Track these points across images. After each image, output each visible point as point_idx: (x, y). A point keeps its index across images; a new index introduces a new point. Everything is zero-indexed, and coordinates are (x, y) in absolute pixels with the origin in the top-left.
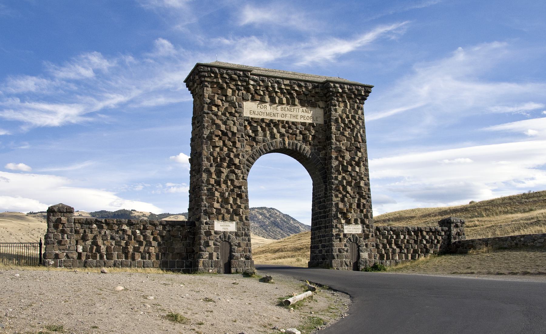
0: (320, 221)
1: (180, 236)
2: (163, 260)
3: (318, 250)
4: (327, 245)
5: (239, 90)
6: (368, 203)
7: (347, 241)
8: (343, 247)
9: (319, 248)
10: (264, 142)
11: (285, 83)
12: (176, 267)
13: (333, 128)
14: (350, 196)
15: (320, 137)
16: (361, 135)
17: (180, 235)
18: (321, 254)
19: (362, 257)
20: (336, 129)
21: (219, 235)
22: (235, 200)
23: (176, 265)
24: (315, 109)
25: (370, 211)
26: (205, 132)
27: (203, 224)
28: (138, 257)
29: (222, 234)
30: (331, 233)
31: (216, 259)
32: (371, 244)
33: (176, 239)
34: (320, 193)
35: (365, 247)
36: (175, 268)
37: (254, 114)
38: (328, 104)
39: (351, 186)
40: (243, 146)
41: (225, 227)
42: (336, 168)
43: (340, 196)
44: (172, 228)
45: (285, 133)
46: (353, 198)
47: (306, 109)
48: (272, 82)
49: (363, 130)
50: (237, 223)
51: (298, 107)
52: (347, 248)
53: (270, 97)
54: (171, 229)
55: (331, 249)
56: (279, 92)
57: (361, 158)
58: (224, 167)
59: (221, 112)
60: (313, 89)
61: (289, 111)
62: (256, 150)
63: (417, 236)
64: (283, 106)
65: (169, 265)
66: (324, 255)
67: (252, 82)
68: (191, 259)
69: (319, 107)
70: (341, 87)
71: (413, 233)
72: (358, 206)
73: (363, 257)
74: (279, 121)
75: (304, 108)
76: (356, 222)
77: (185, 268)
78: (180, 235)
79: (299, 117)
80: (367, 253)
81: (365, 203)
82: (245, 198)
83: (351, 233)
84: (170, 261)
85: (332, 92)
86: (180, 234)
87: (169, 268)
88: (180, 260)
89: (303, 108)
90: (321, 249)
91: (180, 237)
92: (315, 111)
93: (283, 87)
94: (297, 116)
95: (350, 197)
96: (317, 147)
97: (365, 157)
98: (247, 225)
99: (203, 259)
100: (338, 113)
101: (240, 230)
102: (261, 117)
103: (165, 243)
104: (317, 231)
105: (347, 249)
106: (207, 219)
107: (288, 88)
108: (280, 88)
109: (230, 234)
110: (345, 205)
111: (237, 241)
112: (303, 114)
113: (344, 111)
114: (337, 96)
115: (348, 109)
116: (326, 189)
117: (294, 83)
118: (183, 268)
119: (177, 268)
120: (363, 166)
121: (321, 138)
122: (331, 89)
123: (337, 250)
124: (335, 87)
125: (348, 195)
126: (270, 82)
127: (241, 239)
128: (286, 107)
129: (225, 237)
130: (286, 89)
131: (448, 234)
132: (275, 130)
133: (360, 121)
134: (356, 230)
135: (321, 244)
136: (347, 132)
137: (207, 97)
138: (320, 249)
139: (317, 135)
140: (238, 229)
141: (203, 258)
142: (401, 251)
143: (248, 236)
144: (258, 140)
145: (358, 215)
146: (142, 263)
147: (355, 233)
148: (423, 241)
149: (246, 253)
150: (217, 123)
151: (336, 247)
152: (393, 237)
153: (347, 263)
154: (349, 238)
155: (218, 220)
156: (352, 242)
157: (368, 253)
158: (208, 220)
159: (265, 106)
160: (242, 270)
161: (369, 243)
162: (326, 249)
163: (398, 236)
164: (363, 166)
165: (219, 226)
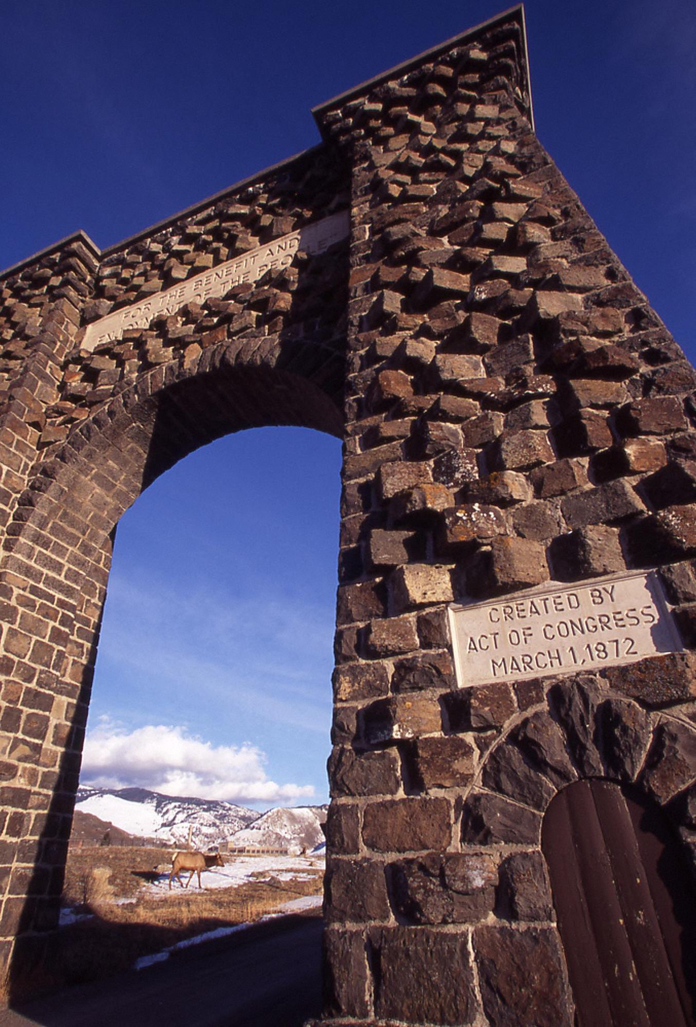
6: (660, 389)
7: (491, 776)
39: (472, 347)
43: (403, 426)
46: (508, 404)
51: (253, 253)
52: (507, 849)
56: (188, 252)
83: (526, 676)
89: (270, 247)
93: (192, 229)
105: (506, 869)
107: (216, 223)
108: (188, 239)
110: (445, 471)
123: (379, 885)
125: (449, 402)
126: (158, 243)
134: (593, 639)
147: (590, 665)
151: (365, 851)
156: (563, 775)
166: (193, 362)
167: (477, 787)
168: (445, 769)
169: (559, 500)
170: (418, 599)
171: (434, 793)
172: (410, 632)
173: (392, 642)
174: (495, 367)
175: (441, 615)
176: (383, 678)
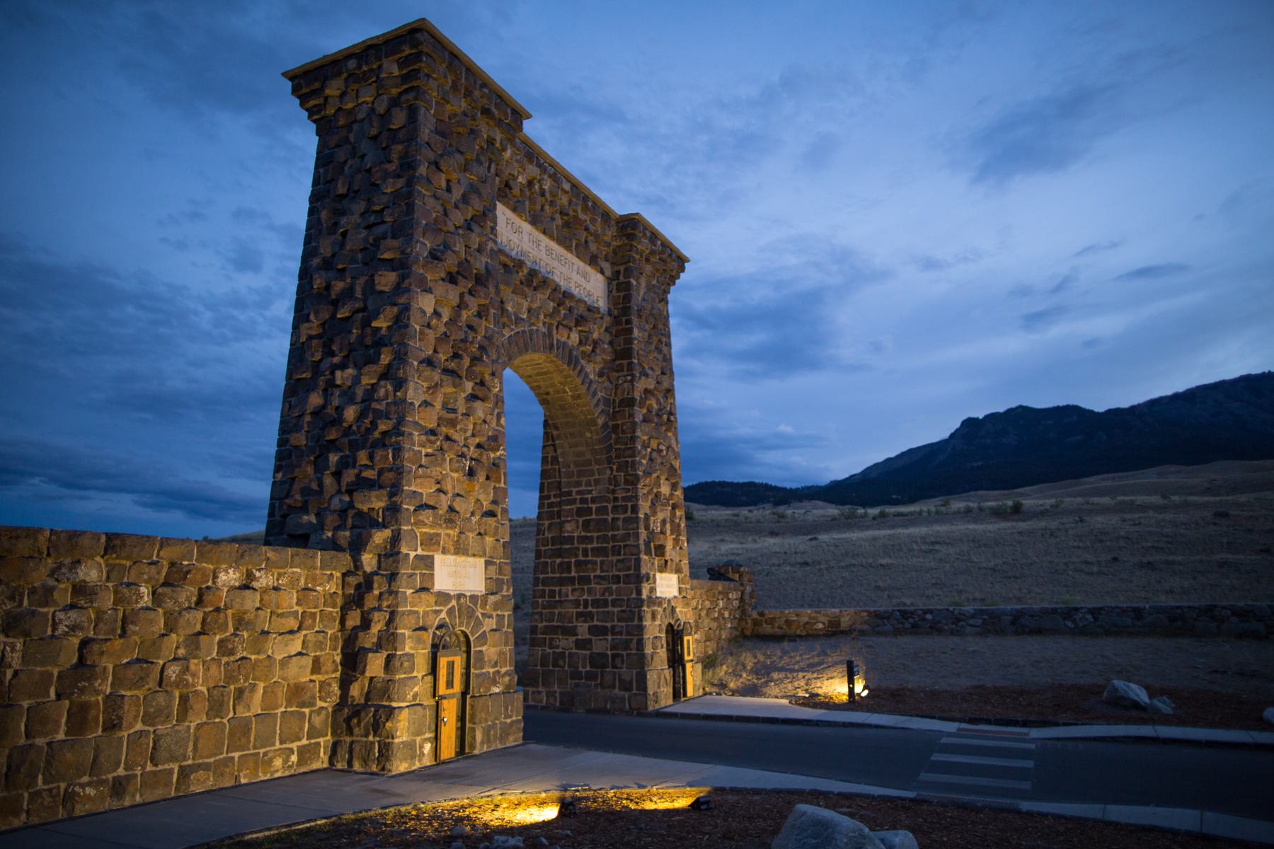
0: (587, 562)
1: (296, 608)
3: (574, 638)
4: (617, 630)
9: (577, 635)
17: (297, 604)
18: (588, 652)
23: (278, 732)
29: (454, 602)
30: (634, 596)
34: (583, 488)
36: (274, 744)
38: (618, 272)
50: (488, 563)
55: (635, 642)
65: (252, 739)
66: (604, 655)
68: (326, 702)
77: (305, 742)
78: (297, 604)
87: (252, 751)
90: (588, 637)
104: (570, 588)
106: (416, 550)
116: (613, 481)
118: (300, 740)
135: (586, 625)
138: (580, 637)
146: (148, 744)
162: (610, 638)
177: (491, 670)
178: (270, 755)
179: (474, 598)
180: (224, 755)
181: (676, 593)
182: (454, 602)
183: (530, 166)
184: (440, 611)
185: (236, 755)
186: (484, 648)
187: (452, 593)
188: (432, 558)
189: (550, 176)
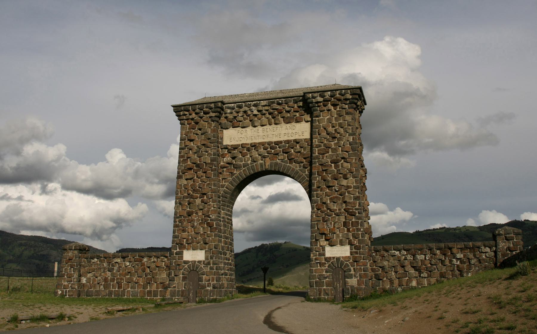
1: (164, 266)
2: (148, 289)
5: (213, 121)
7: (328, 267)
8: (324, 273)
10: (244, 167)
11: (263, 104)
12: (159, 297)
13: (316, 142)
14: (334, 214)
15: (305, 153)
16: (349, 143)
19: (348, 284)
20: (318, 142)
21: (187, 265)
22: (204, 228)
23: (159, 294)
24: (301, 123)
25: (360, 229)
26: (179, 167)
27: (173, 255)
28: (128, 287)
29: (191, 263)
31: (183, 289)
32: (361, 268)
33: (160, 269)
35: (352, 272)
36: (158, 297)
37: (234, 141)
40: (215, 175)
41: (194, 257)
42: (316, 185)
44: (157, 259)
45: (266, 154)
47: (289, 125)
48: (249, 106)
49: (353, 138)
50: (206, 251)
51: (281, 125)
52: (329, 273)
53: (251, 121)
54: (155, 260)
57: (348, 169)
58: (194, 198)
59: (196, 145)
60: (296, 104)
61: (271, 131)
62: (235, 176)
63: (445, 255)
64: (265, 127)
67: (229, 111)
69: (305, 120)
70: (321, 96)
71: (438, 252)
72: (345, 224)
73: (349, 285)
74: (259, 143)
75: (288, 125)
76: (342, 244)
78: (164, 265)
79: (282, 136)
80: (356, 279)
81: (353, 220)
82: (215, 226)
83: (334, 256)
84: (154, 291)
85: (312, 103)
86: (164, 264)
87: (152, 297)
88: (163, 290)
89: (286, 126)
91: (164, 267)
92: (301, 126)
93: (260, 108)
94: (280, 135)
95: (334, 215)
96: (302, 164)
97: (354, 168)
98: (215, 253)
99: (170, 289)
100: (321, 123)
101: (208, 259)
102: (240, 143)
103: (151, 273)
106: (177, 250)
108: (259, 111)
109: (198, 264)
111: (204, 270)
112: (286, 131)
113: (329, 120)
114: (319, 106)
115: (334, 118)
117: (273, 103)
119: (160, 297)
120: (352, 177)
121: (306, 153)
122: (309, 101)
124: (313, 97)
127: (209, 268)
128: (267, 128)
129: (193, 267)
130: (267, 110)
131: (494, 249)
132: (255, 154)
133: (349, 127)
136: (332, 143)
137: (184, 133)
139: (303, 151)
140: (206, 258)
141: (170, 288)
142: (420, 274)
143: (215, 265)
144: (237, 166)
145: (344, 235)
148: (453, 261)
149: (213, 282)
150: (190, 156)
152: (406, 257)
153: (326, 292)
154: (331, 263)
155: (187, 250)
157: (357, 280)
158: (178, 250)
159: (246, 131)
160: (207, 299)
161: (358, 267)
163: (414, 256)
164: (351, 178)
165: (189, 255)
166: (268, 165)
167: (327, 267)
168: (324, 266)
169: (341, 234)
170: (322, 245)
171: (322, 268)
172: (321, 249)
173: (318, 250)
174: (337, 206)
175: (325, 247)
176: (317, 254)
177: (207, 283)
178: (157, 299)
179: (199, 262)
180: (146, 297)
181: (348, 254)
182: (191, 263)
183: (242, 109)
184: (186, 265)
185: (149, 298)
186: (204, 276)
187: (190, 261)
188: (183, 251)
189: (253, 106)
